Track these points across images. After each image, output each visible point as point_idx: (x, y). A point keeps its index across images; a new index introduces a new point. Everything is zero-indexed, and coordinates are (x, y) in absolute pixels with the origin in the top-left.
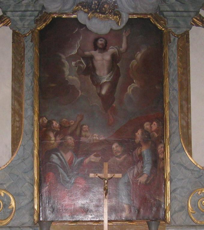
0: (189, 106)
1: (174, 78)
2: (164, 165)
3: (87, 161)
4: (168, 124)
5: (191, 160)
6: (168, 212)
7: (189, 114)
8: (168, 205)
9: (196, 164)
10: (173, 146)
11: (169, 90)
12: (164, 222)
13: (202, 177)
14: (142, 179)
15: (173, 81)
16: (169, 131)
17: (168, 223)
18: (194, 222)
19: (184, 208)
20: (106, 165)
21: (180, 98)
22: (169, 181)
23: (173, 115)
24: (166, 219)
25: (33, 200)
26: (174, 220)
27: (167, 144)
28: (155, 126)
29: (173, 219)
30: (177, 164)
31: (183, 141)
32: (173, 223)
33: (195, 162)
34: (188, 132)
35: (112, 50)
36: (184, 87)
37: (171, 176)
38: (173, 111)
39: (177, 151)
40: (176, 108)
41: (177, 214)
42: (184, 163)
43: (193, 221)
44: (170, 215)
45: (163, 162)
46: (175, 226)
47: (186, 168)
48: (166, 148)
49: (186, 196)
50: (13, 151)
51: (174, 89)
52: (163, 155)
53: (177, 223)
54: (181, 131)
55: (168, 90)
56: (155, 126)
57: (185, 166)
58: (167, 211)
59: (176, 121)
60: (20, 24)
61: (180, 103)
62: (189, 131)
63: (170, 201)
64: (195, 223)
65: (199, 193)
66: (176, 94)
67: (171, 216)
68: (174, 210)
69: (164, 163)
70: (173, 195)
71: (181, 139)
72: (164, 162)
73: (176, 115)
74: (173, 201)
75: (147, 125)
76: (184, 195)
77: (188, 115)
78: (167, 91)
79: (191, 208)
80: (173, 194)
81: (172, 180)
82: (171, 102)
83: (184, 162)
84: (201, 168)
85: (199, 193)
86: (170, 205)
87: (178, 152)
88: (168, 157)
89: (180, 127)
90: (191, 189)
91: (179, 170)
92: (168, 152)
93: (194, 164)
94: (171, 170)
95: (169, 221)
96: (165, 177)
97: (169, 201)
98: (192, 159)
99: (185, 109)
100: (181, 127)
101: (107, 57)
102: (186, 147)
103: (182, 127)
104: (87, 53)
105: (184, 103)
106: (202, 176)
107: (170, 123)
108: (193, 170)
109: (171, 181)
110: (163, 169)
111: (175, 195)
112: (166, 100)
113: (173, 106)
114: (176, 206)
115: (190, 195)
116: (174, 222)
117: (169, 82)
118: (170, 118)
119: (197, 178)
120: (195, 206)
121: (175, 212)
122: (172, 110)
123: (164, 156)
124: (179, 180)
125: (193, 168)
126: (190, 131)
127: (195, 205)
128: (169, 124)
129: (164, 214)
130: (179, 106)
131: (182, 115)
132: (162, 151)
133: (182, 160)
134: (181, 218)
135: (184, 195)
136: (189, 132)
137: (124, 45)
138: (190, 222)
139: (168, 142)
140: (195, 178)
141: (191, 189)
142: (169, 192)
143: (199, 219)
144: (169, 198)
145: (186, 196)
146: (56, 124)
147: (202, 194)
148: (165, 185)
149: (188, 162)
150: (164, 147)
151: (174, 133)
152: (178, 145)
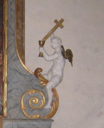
0: (24, 24)
1: (11, 1)
2: (3, 70)
4: (6, 38)
5: (24, 67)
6: (5, 108)
7: (23, 30)
8: (5, 102)
9: (28, 70)
10: (10, 56)
11: (8, 11)
12: (2, 116)
13: (32, 81)
15: (11, 3)
16: (7, 43)
17: (5, 117)
18: (26, 117)
19: (18, 105)
21: (16, 17)
22: (6, 84)
23: (11, 31)
24: (3, 114)
26: (9, 115)
27: (5, 54)
29: (8, 114)
30: (13, 70)
31: (18, 52)
32: (9, 117)
33: (27, 69)
34: (22, 45)
36: (20, 9)
37: (8, 79)
38: (10, 28)
39: (13, 60)
40: (13, 25)
41: (12, 110)
42: (18, 70)
43: (25, 116)
44: (7, 111)
45: (2, 68)
46: (10, 119)
47: (20, 73)
48: (4, 57)
49: (19, 96)
51: (12, 10)
52: (2, 62)
53: (12, 117)
54: (17, 44)
55: (7, 11)
57: (19, 71)
58: (4, 107)
59: (13, 36)
61: (16, 21)
62: (23, 44)
63: (7, 100)
64: (26, 117)
65: (30, 93)
66: (13, 14)
67: (7, 111)
68: (9, 107)
69: (3, 69)
70: (9, 94)
71: (16, 50)
72: (3, 68)
73: (13, 31)
74: (9, 100)
76: (18, 94)
77: (22, 31)
78: (6, 11)
79: (23, 105)
80: (9, 93)
81: (9, 83)
82: (9, 21)
83: (19, 68)
84: (32, 73)
85: (30, 93)
86: (6, 102)
87: (14, 60)
88: (6, 64)
89: (16, 40)
90: (23, 90)
91: (14, 75)
92: (5, 60)
93: (26, 70)
94: (8, 75)
95: (6, 115)
96: (3, 80)
97: (5, 99)
98: (25, 66)
99: (20, 26)
100: (16, 40)
102: (20, 57)
103: (18, 41)
105: (19, 21)
106: (32, 80)
107: (8, 37)
108: (26, 75)
109: (8, 83)
111: (11, 95)
112: (5, 18)
113: (11, 24)
114: (11, 104)
115: (23, 95)
116: (10, 116)
117: (8, 4)
118: (8, 33)
119: (29, 81)
120: (26, 104)
121: (11, 108)
122: (10, 27)
123: (3, 63)
124: (14, 82)
125: (25, 74)
126: (24, 43)
127: (26, 103)
128: (7, 39)
129: (1, 109)
130: (15, 24)
131: (18, 31)
132: (1, 60)
133: (16, 67)
134: (15, 113)
135: (18, 94)
136: (23, 44)
138: (22, 117)
139: (6, 52)
140: (27, 81)
141: (23, 90)
142: (6, 92)
143: (30, 114)
144: (6, 97)
145: (19, 96)
147: (32, 94)
148: (3, 86)
149: (22, 68)
150: (3, 56)
151: (11, 45)
152: (14, 55)
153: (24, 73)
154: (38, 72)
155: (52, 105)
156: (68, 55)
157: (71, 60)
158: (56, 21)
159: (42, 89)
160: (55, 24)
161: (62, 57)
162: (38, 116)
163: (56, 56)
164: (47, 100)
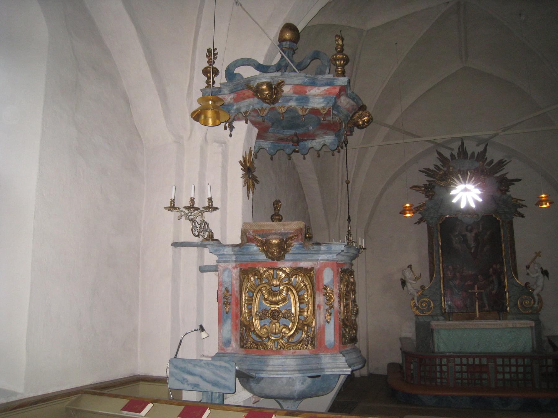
3: (466, 284)
14: (494, 292)
19: (516, 305)
20: (476, 286)
25: (441, 303)
28: (498, 266)
35: (475, 231)
50: (431, 280)
56: (498, 266)
60: (431, 222)
75: (494, 266)
101: (473, 235)
104: (464, 233)
110: (504, 287)
127: (521, 304)
137: (481, 229)
146: (450, 267)
153: (518, 286)
154: (527, 284)
155: (538, 304)
156: (545, 273)
157: (548, 276)
158: (536, 253)
159: (531, 294)
160: (535, 255)
161: (541, 275)
162: (530, 311)
163: (537, 274)
164: (535, 301)
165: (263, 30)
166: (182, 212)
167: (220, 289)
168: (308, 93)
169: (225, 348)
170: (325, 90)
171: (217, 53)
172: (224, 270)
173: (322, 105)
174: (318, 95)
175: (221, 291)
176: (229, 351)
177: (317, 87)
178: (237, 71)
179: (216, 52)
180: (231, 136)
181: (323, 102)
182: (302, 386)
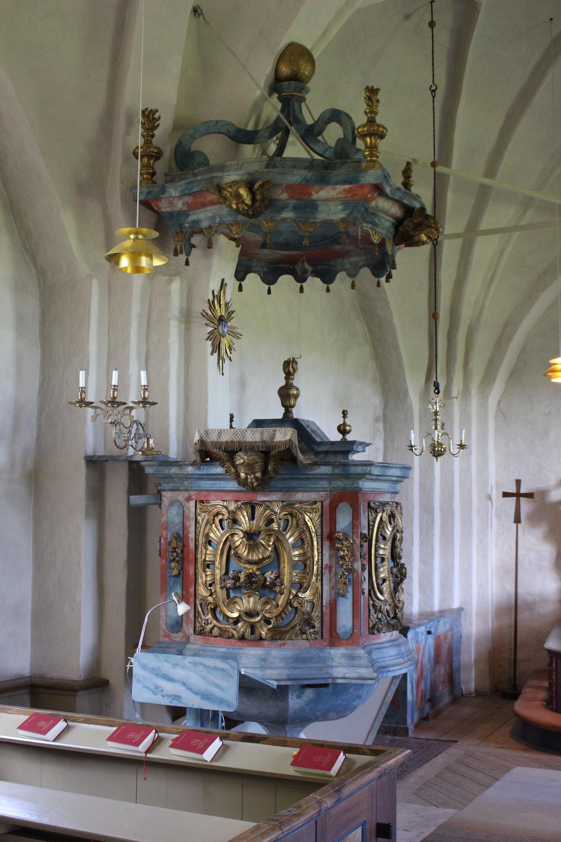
165: (244, 67)
166: (96, 407)
167: (165, 536)
168: (315, 196)
169: (172, 634)
170: (344, 190)
171: (159, 117)
172: (172, 504)
173: (342, 215)
174: (333, 199)
175: (166, 539)
176: (178, 639)
177: (330, 187)
178: (196, 146)
179: (156, 116)
180: (187, 263)
181: (342, 210)
182: (298, 701)
